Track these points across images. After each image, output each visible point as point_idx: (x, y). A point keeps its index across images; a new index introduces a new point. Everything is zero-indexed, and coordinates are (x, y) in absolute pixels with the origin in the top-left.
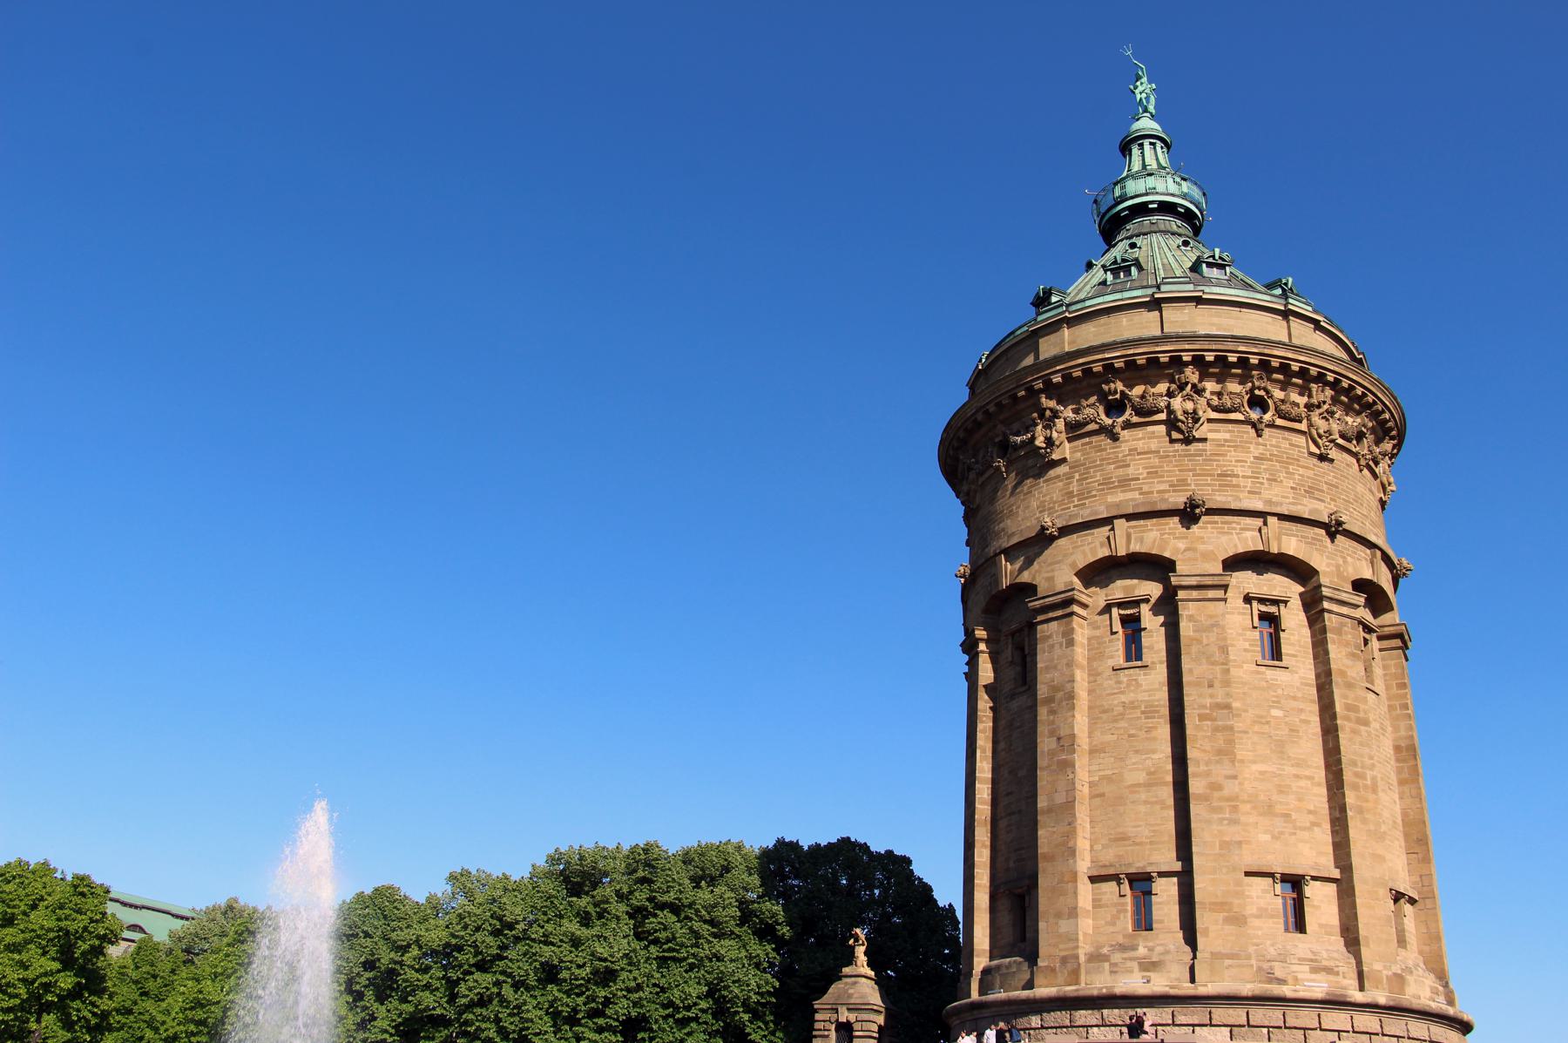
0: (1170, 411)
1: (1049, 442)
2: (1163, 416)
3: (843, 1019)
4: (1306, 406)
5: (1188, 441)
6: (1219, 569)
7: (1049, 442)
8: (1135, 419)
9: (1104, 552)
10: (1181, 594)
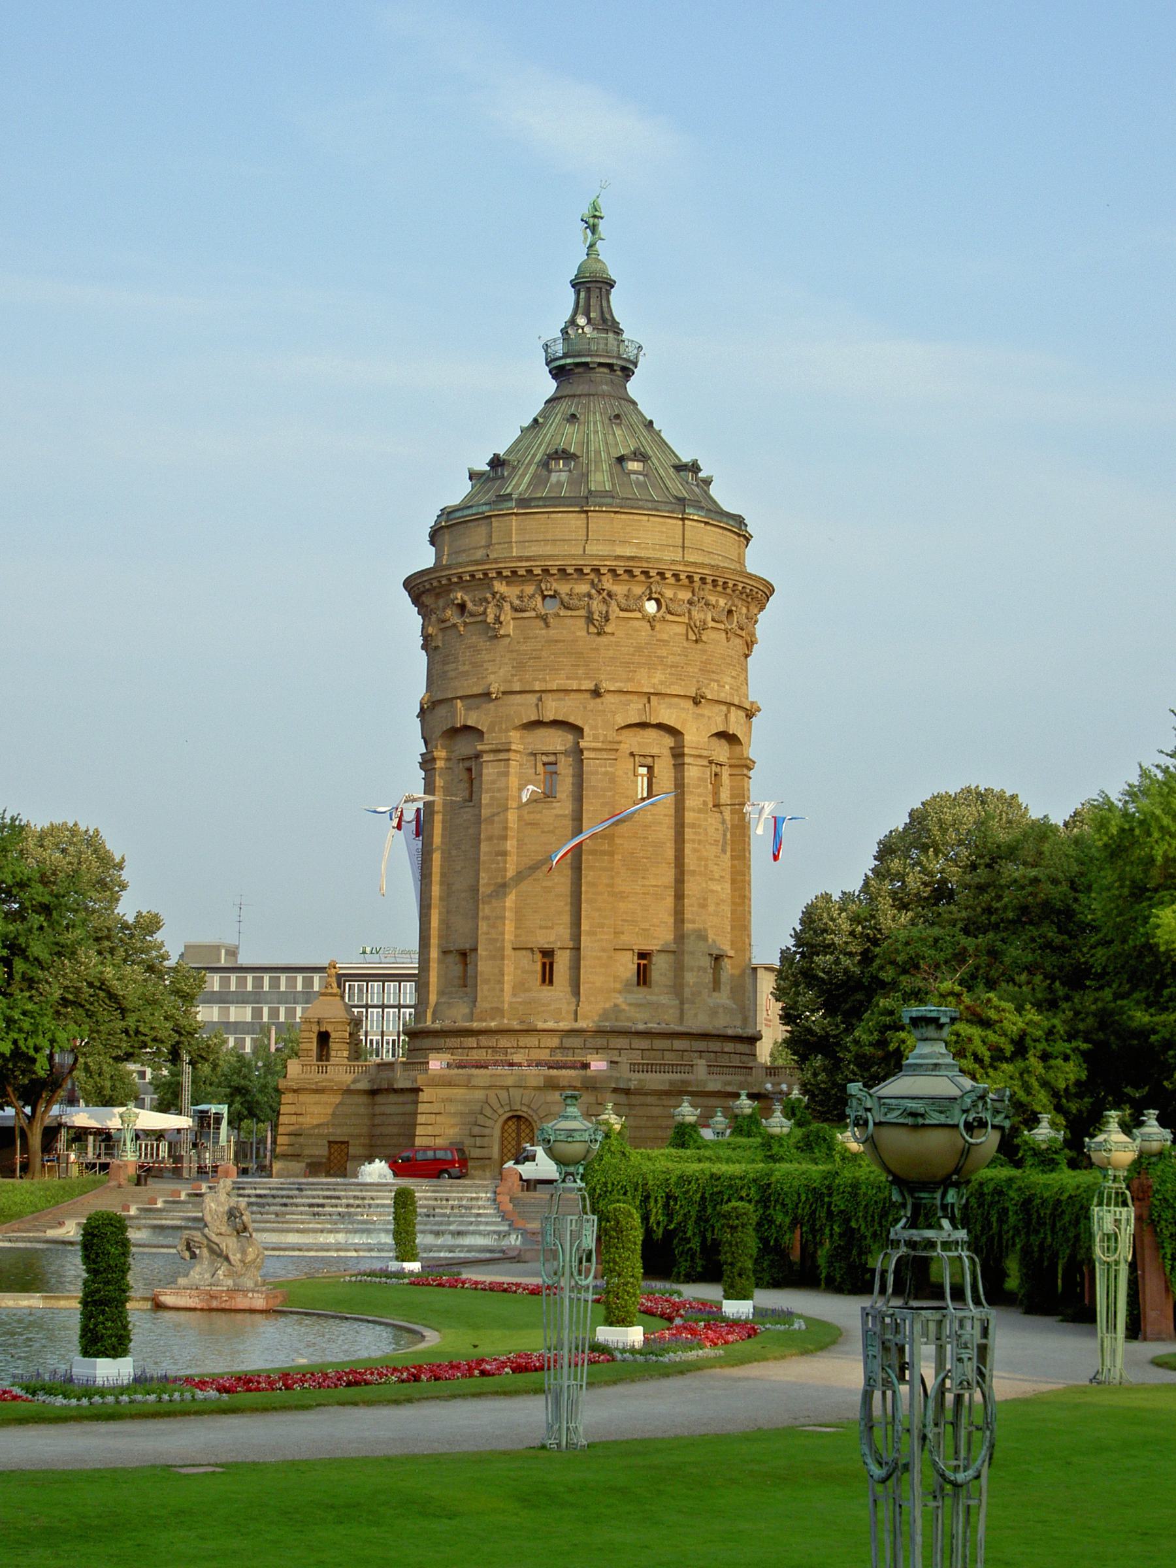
0: (590, 613)
1: (497, 619)
2: (583, 612)
3: (323, 1029)
4: (690, 603)
5: (599, 634)
7: (497, 619)
8: (563, 612)
9: (533, 718)
10: (586, 754)
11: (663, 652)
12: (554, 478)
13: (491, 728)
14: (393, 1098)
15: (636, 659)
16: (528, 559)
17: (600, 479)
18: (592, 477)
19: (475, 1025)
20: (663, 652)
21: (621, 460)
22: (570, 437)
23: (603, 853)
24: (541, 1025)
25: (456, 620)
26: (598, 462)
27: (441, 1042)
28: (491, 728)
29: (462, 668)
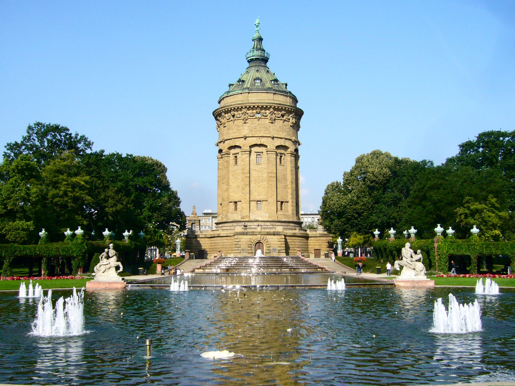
6: (275, 148)
8: (263, 117)
11: (285, 128)
12: (256, 84)
13: (244, 146)
14: (219, 238)
15: (279, 129)
16: (254, 103)
17: (268, 85)
18: (266, 84)
19: (242, 220)
20: (285, 128)
21: (271, 81)
22: (258, 75)
23: (273, 177)
24: (260, 219)
25: (232, 119)
26: (266, 81)
27: (241, 224)
28: (244, 146)
29: (234, 131)
